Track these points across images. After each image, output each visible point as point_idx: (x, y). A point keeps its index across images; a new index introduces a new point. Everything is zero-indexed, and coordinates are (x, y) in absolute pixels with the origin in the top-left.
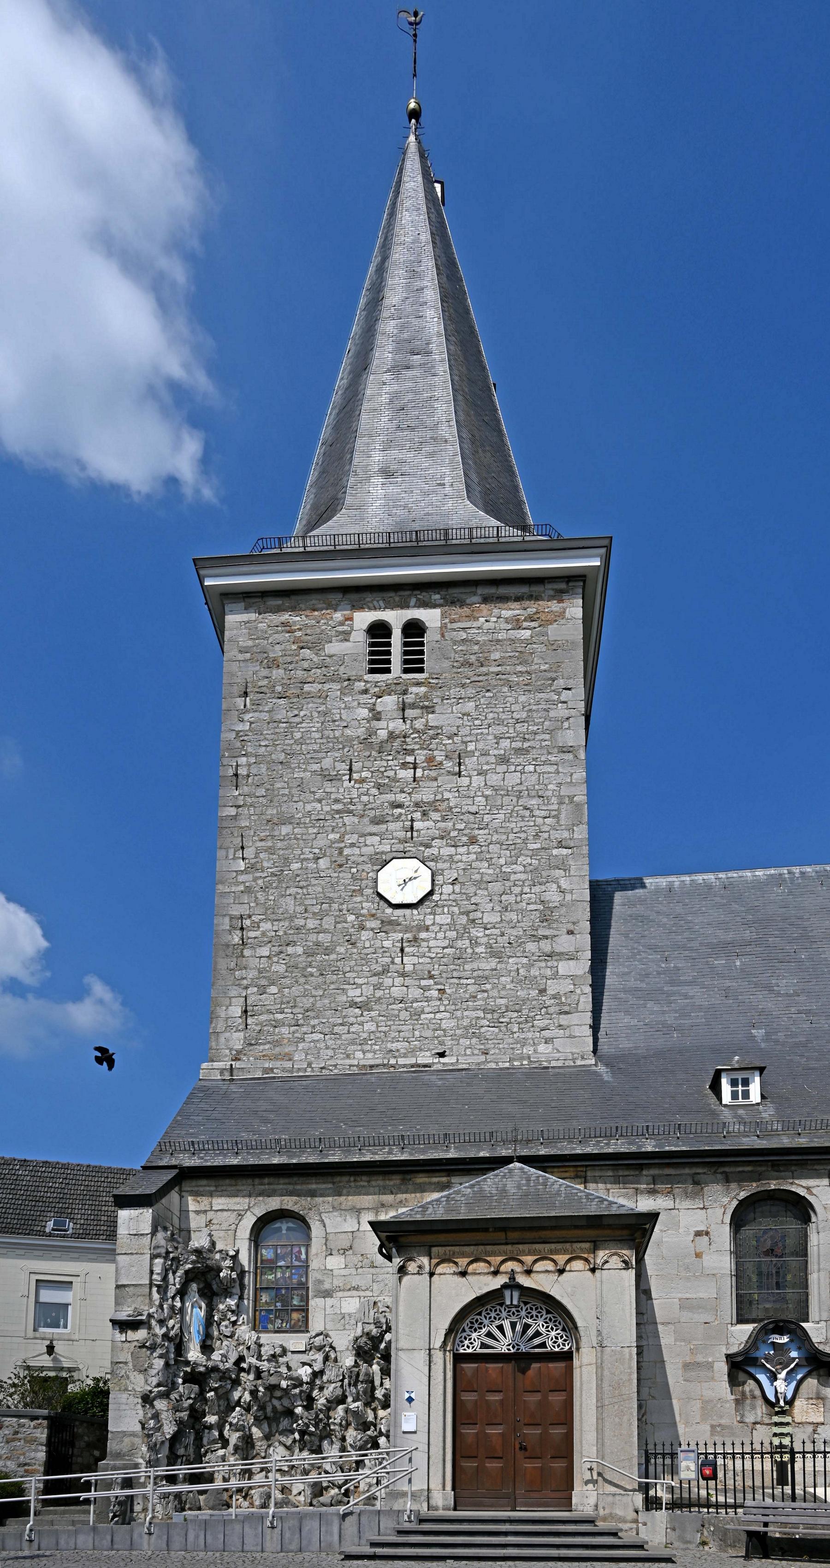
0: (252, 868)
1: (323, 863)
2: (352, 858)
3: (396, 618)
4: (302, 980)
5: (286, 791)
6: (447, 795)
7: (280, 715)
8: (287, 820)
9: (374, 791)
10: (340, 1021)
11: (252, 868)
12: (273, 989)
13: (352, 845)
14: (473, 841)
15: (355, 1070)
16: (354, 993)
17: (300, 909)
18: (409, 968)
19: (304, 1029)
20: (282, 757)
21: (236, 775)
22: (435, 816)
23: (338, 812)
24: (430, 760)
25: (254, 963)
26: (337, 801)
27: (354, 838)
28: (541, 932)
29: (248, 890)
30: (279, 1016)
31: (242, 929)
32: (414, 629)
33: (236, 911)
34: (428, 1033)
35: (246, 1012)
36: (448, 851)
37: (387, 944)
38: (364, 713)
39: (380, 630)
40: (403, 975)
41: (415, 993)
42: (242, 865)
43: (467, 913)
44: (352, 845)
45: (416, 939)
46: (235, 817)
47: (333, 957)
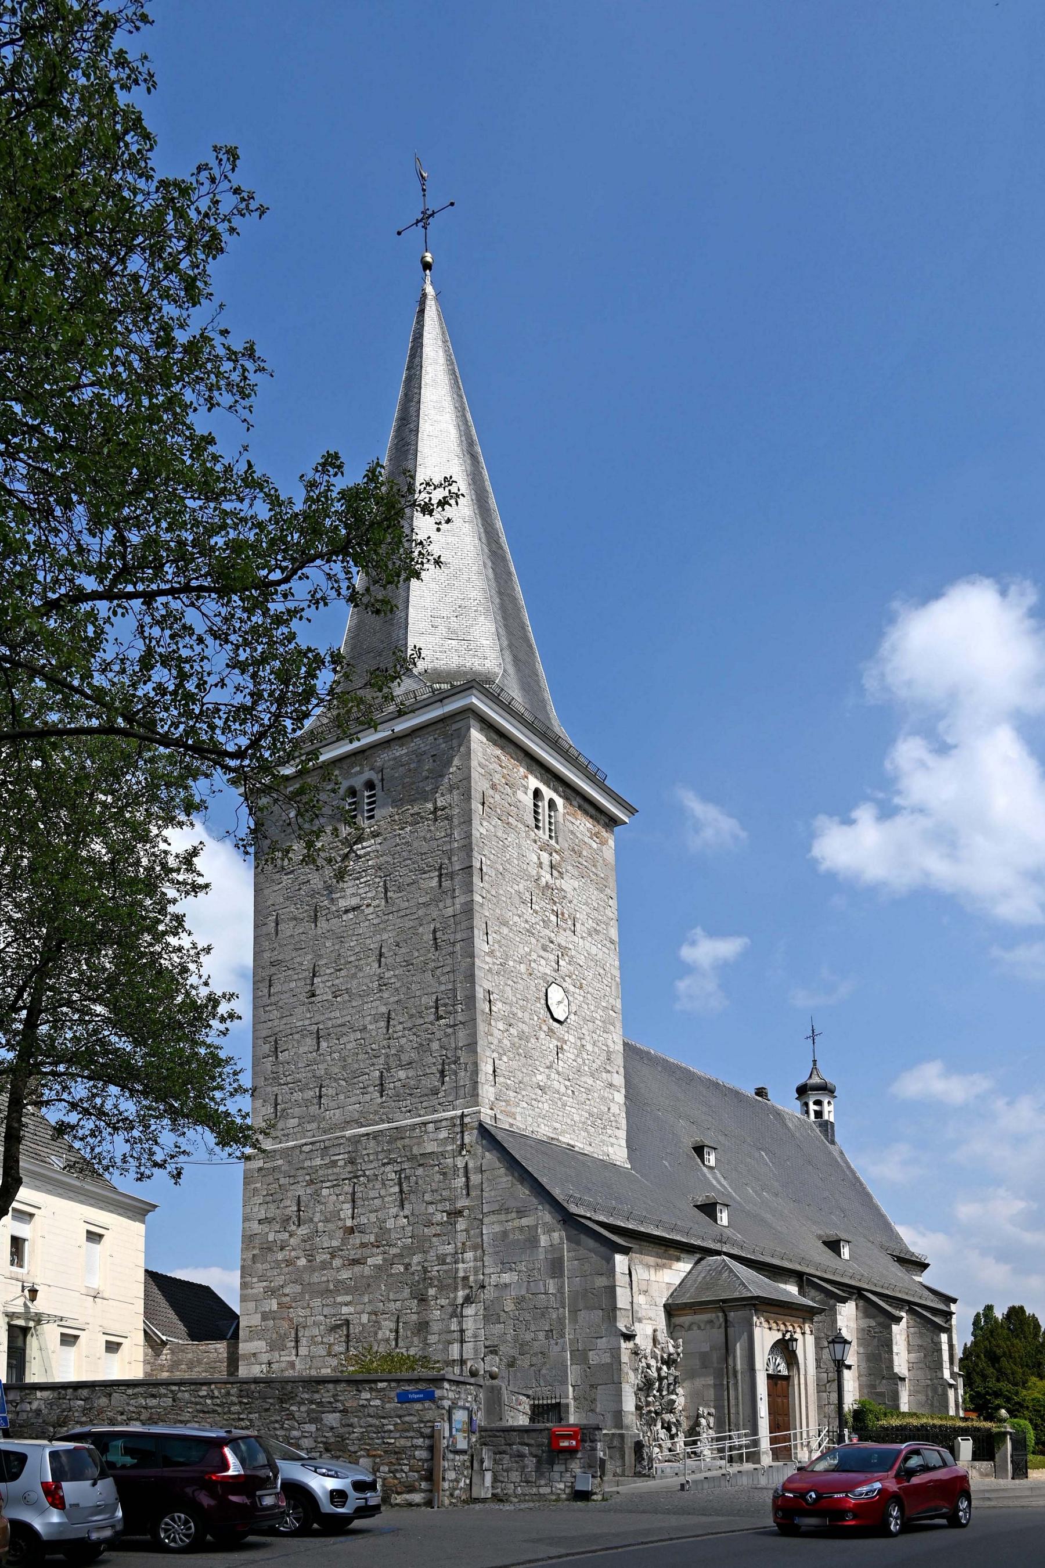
0: (491, 953)
1: (523, 968)
2: (536, 972)
3: (548, 793)
4: (517, 1058)
5: (504, 899)
6: (571, 946)
7: (500, 834)
8: (505, 924)
9: (541, 923)
10: (534, 1097)
11: (491, 953)
12: (505, 1059)
13: (535, 961)
14: (581, 987)
15: (545, 1139)
16: (540, 1078)
17: (514, 1000)
18: (560, 1069)
19: (520, 1096)
20: (501, 870)
21: (481, 870)
22: (567, 958)
23: (528, 931)
24: (563, 914)
25: (496, 1032)
26: (527, 921)
27: (534, 956)
28: (608, 1068)
29: (490, 970)
30: (509, 1082)
31: (490, 1001)
32: (552, 804)
33: (487, 986)
34: (569, 1121)
35: (494, 1071)
36: (572, 988)
37: (551, 1046)
38: (535, 859)
39: (537, 793)
40: (558, 1073)
41: (563, 1090)
42: (486, 948)
43: (580, 1039)
44: (535, 961)
45: (562, 1048)
46: (482, 905)
47: (530, 1045)
